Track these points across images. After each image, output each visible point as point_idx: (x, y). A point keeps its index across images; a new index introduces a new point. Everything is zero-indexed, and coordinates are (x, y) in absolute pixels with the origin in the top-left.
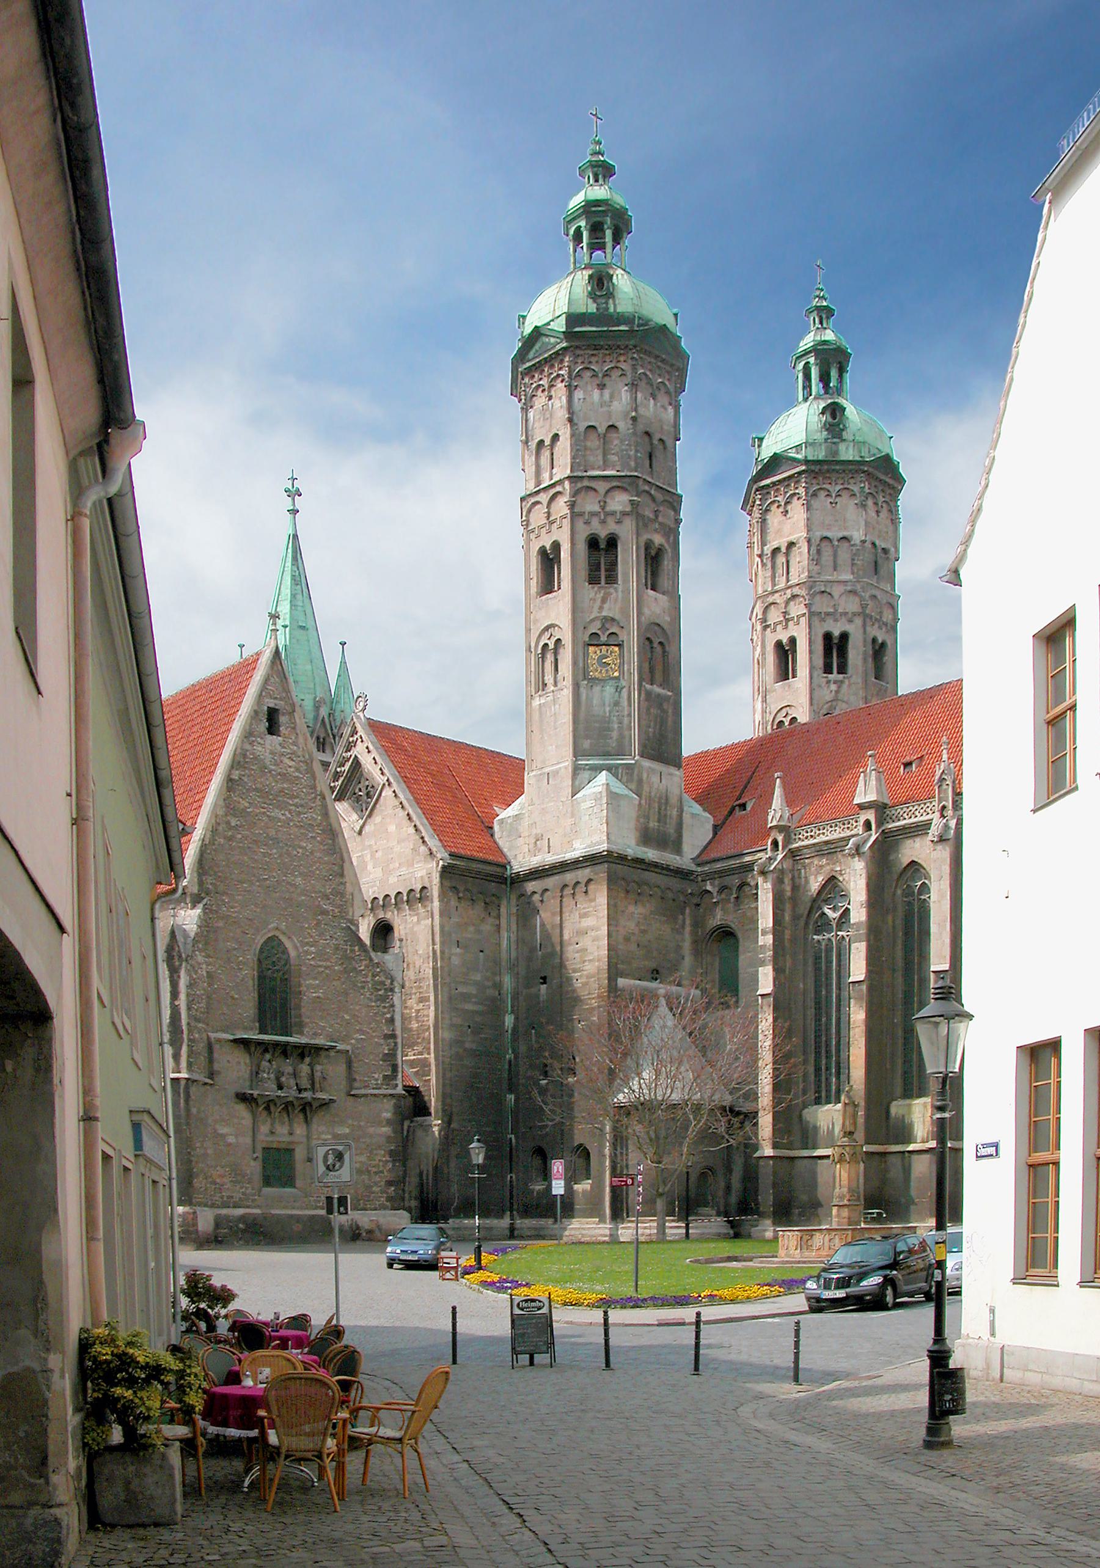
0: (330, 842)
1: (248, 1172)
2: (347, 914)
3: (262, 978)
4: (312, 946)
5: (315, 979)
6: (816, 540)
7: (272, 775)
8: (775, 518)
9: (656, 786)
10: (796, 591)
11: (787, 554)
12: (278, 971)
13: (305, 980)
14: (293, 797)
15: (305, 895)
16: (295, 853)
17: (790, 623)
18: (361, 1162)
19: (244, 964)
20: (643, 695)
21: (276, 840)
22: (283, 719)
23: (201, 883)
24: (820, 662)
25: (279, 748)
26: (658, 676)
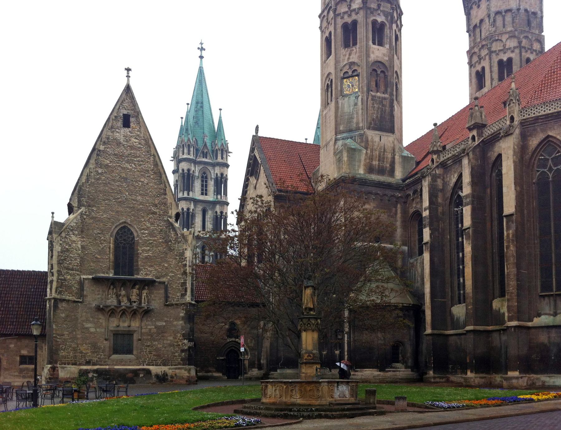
0: (158, 178)
1: (102, 347)
2: (168, 213)
3: (116, 248)
4: (145, 230)
5: (147, 246)
6: (492, 15)
7: (125, 147)
8: (474, 12)
9: (376, 144)
10: (484, 43)
11: (480, 26)
12: (128, 244)
13: (141, 247)
14: (136, 157)
15: (143, 205)
16: (137, 184)
17: (482, 61)
18: (170, 340)
19: (105, 241)
20: (370, 98)
21: (125, 179)
22: (132, 119)
23: (79, 201)
24: (496, 76)
25: (129, 133)
26: (382, 88)
